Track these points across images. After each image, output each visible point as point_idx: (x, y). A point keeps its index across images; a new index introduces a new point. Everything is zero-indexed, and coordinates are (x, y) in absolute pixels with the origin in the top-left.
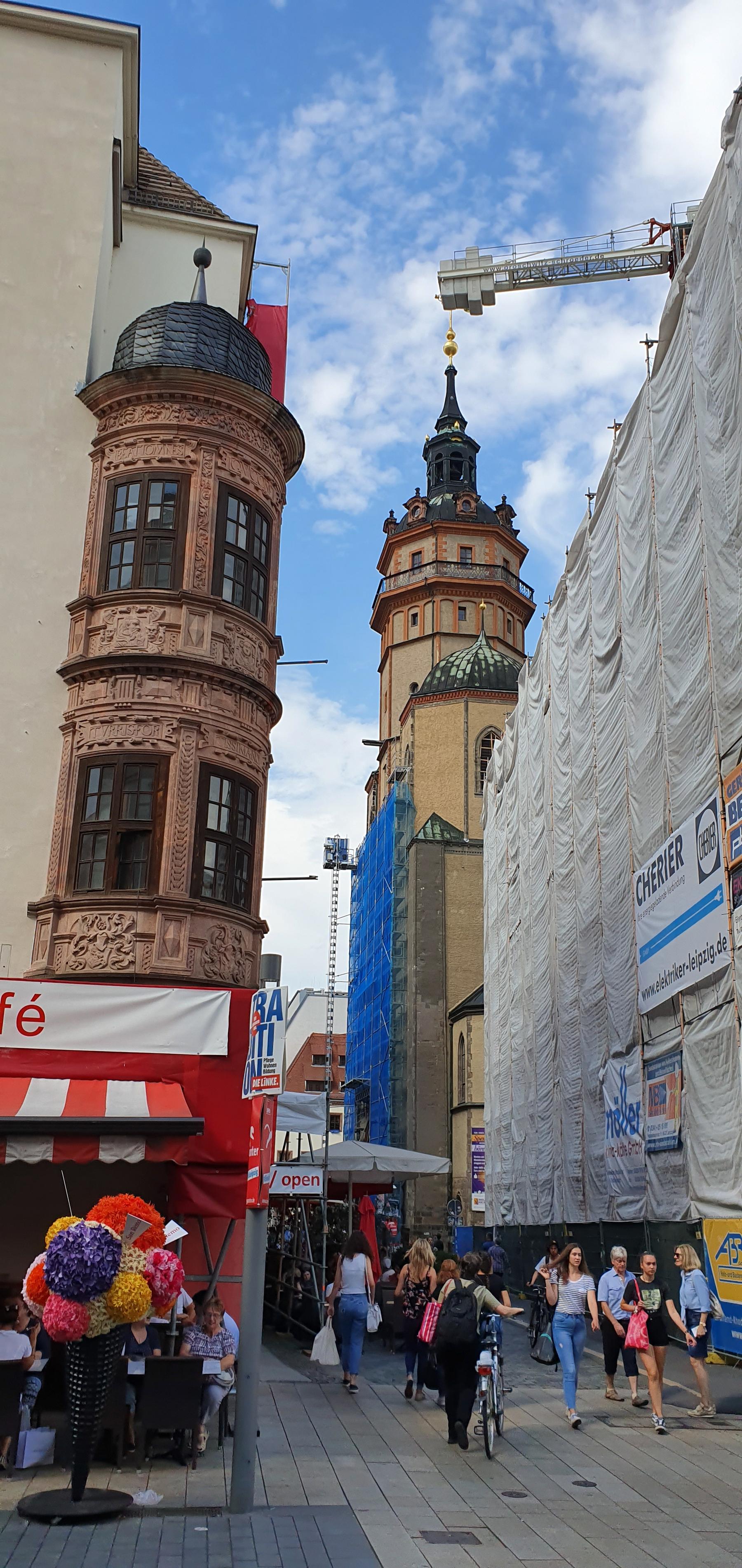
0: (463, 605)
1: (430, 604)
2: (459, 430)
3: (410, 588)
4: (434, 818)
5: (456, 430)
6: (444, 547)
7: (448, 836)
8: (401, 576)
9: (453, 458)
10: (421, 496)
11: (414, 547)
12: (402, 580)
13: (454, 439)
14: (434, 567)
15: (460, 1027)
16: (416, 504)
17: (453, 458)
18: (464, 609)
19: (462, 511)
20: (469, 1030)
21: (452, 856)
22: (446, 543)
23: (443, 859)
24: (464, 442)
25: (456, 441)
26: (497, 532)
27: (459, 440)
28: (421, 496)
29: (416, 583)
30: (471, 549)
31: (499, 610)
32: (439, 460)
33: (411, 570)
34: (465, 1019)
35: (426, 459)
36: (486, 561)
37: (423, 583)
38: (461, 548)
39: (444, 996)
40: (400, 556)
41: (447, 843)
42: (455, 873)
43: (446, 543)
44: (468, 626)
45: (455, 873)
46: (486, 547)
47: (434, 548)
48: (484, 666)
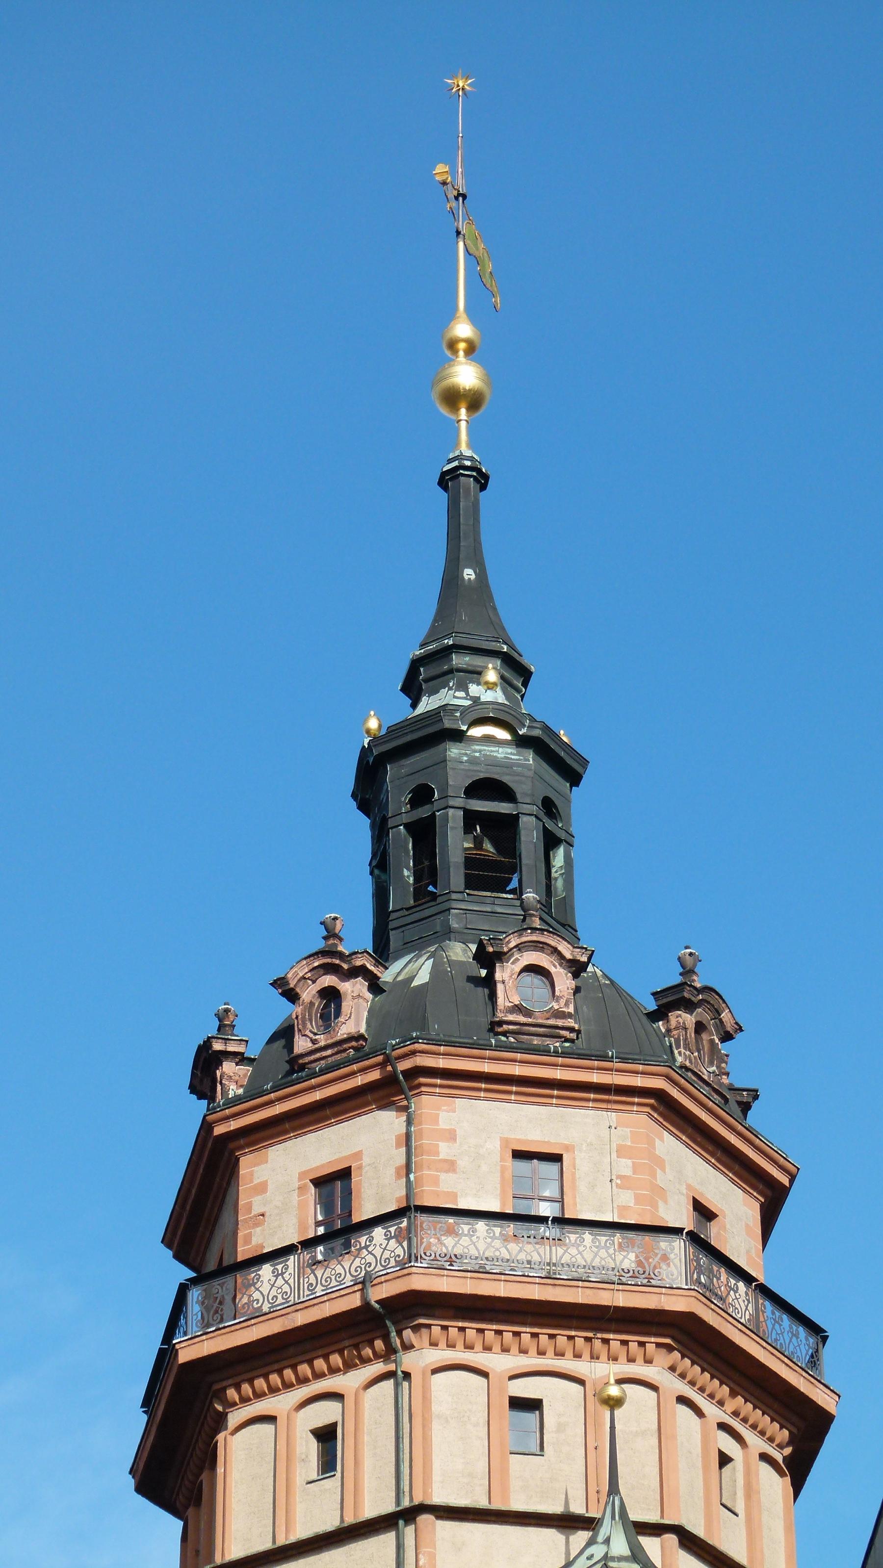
0: (525, 1389)
1: (388, 1385)
2: (498, 696)
3: (301, 1319)
5: (488, 696)
6: (445, 1150)
8: (266, 1270)
9: (480, 806)
13: (477, 732)
14: (398, 1237)
16: (329, 980)
17: (480, 806)
18: (533, 1405)
19: (518, 1009)
22: (451, 1136)
24: (521, 742)
25: (488, 739)
27: (502, 734)
29: (330, 1295)
30: (557, 1158)
31: (683, 1410)
32: (423, 812)
33: (309, 1244)
35: (364, 806)
36: (623, 1209)
37: (355, 1301)
38: (519, 1155)
40: (262, 1188)
44: (554, 1478)
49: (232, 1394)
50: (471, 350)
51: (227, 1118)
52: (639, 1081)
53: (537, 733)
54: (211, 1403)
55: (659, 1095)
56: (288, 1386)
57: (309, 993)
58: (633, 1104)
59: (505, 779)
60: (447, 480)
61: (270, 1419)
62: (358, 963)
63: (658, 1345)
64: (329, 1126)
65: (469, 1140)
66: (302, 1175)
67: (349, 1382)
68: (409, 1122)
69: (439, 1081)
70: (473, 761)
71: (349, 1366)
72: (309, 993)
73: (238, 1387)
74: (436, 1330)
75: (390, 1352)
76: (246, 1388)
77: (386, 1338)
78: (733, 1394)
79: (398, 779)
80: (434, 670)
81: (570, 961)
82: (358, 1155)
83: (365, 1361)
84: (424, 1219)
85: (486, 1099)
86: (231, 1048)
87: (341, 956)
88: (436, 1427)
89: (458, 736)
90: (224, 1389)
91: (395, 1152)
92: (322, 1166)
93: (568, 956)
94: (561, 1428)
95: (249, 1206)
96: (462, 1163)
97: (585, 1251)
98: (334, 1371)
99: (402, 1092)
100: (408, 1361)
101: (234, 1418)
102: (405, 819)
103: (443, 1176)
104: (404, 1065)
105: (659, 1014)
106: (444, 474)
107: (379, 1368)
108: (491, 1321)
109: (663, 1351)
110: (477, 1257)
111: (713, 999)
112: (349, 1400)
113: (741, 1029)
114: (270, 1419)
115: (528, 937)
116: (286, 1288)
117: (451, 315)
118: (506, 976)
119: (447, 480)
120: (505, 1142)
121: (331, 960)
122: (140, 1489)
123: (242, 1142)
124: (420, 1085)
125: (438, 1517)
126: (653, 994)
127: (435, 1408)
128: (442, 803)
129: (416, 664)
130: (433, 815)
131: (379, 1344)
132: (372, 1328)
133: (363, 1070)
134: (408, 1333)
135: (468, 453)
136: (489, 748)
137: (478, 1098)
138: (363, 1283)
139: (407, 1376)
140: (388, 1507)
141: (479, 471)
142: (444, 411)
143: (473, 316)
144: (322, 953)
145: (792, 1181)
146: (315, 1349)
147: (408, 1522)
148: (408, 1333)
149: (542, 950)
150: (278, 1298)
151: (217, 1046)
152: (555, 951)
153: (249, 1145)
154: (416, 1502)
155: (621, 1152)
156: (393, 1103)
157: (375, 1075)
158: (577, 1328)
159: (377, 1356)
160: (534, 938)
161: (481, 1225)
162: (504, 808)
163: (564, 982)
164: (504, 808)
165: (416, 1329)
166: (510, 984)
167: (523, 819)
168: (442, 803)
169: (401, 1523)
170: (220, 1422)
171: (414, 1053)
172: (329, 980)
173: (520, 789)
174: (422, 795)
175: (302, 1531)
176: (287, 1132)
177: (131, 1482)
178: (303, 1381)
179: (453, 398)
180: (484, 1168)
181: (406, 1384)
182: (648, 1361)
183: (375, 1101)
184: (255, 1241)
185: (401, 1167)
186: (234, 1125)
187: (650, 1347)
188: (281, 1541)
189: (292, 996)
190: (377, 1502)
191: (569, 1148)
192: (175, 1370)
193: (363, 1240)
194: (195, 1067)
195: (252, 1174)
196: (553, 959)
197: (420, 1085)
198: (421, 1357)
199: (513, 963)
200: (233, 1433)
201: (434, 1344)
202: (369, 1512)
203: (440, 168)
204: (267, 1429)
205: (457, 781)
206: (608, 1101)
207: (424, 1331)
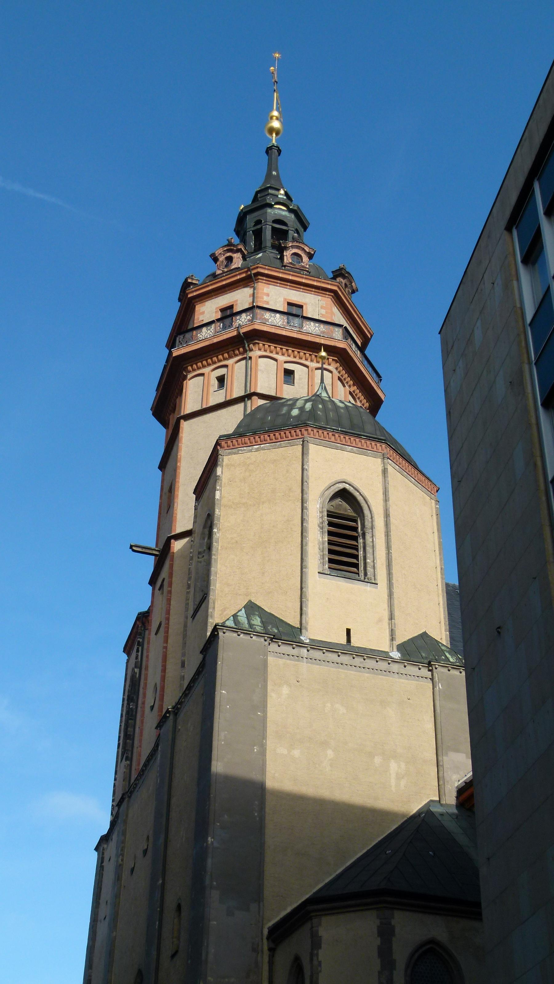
1: (244, 362)
4: (252, 608)
7: (276, 631)
8: (204, 329)
11: (223, 300)
12: (205, 333)
15: (298, 943)
16: (228, 254)
20: (316, 943)
21: (281, 661)
22: (268, 295)
23: (265, 664)
24: (290, 211)
27: (285, 208)
31: (339, 383)
32: (259, 227)
33: (218, 320)
34: (308, 926)
39: (258, 896)
40: (203, 313)
41: (274, 638)
42: (285, 690)
43: (268, 295)
45: (285, 690)
48: (330, 406)
49: (190, 368)
50: (277, 119)
51: (193, 292)
52: (329, 287)
53: (296, 208)
54: (182, 372)
55: (334, 292)
56: (209, 365)
57: (222, 258)
58: (326, 294)
59: (285, 220)
60: (269, 150)
61: (202, 375)
62: (239, 247)
63: (333, 360)
64: (227, 294)
65: (275, 296)
66: (216, 308)
67: (230, 362)
68: (254, 289)
69: (265, 278)
70: (275, 214)
71: (230, 357)
72: (222, 258)
73: (192, 366)
74: (261, 345)
75: (245, 351)
76: (195, 366)
77: (244, 348)
78: (354, 385)
79: (250, 221)
80: (263, 194)
81: (308, 253)
83: (236, 355)
84: (258, 311)
85: (279, 286)
86: (194, 282)
87: (234, 246)
88: (259, 373)
89: (271, 206)
90: (187, 367)
93: (308, 251)
94: (300, 379)
95: (198, 319)
97: (311, 327)
98: (225, 359)
99: (253, 281)
100: (250, 354)
101: (189, 376)
102: (253, 229)
104: (253, 272)
105: (334, 278)
106: (268, 148)
107: (240, 357)
108: (279, 344)
109: (334, 362)
110: (275, 323)
111: (350, 278)
112: (230, 367)
113: (357, 290)
114: (202, 375)
115: (294, 244)
116: (211, 333)
117: (272, 110)
118: (287, 254)
119: (269, 150)
120: (285, 299)
121: (230, 247)
122: (154, 414)
123: (197, 300)
124: (258, 279)
125: (259, 398)
126: (332, 272)
127: (259, 368)
128: (265, 223)
129: (257, 193)
130: (262, 227)
131: (241, 349)
132: (240, 344)
133: (240, 274)
134: (251, 346)
135: (275, 144)
136: (280, 211)
137: (277, 286)
138: (238, 328)
139: (250, 358)
140: (242, 393)
141: (278, 148)
142: (268, 135)
143: (278, 109)
144: (228, 245)
145: (371, 336)
146: (219, 352)
147: (248, 399)
148: (251, 346)
149: (299, 249)
150: (207, 337)
151: (189, 281)
152: (303, 249)
153: (199, 301)
154: (252, 391)
155: (322, 307)
156: (249, 286)
157: (244, 275)
158: (307, 351)
159: (240, 354)
160: (297, 244)
161: (278, 315)
162: (284, 228)
163: (305, 259)
164: (284, 228)
165: (254, 344)
166: (289, 256)
167: (290, 232)
168: (265, 223)
169: (246, 399)
170: (185, 378)
171: (257, 267)
172: (228, 254)
173: (289, 224)
174: (258, 222)
175: (212, 403)
176: (212, 296)
177: (151, 412)
178: (214, 363)
179: (271, 130)
181: (250, 361)
182: (329, 364)
183: (243, 285)
184: (201, 319)
186: (195, 294)
187: (330, 360)
188: (204, 407)
189: (216, 260)
190: (238, 392)
191: (306, 304)
192: (171, 359)
193: (238, 318)
194: (181, 292)
195: (200, 310)
196: (303, 252)
197: (258, 279)
198: (256, 353)
200: (189, 380)
201: (260, 349)
202: (235, 395)
203: (272, 68)
204: (201, 378)
205: (270, 219)
206: (318, 292)
207: (257, 345)
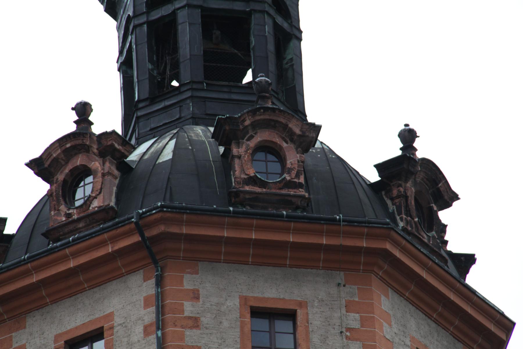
6: (189, 308)
10: (98, 128)
16: (79, 161)
19: (253, 180)
22: (195, 296)
26: (387, 255)
28: (97, 129)
30: (290, 315)
38: (257, 313)
46: (349, 307)
47: (149, 315)
82: (110, 316)
91: (143, 312)
92: (76, 328)
96: (205, 320)
103: (188, 332)
180: (226, 324)
185: (151, 325)
191: (303, 304)
199: (248, 140)
